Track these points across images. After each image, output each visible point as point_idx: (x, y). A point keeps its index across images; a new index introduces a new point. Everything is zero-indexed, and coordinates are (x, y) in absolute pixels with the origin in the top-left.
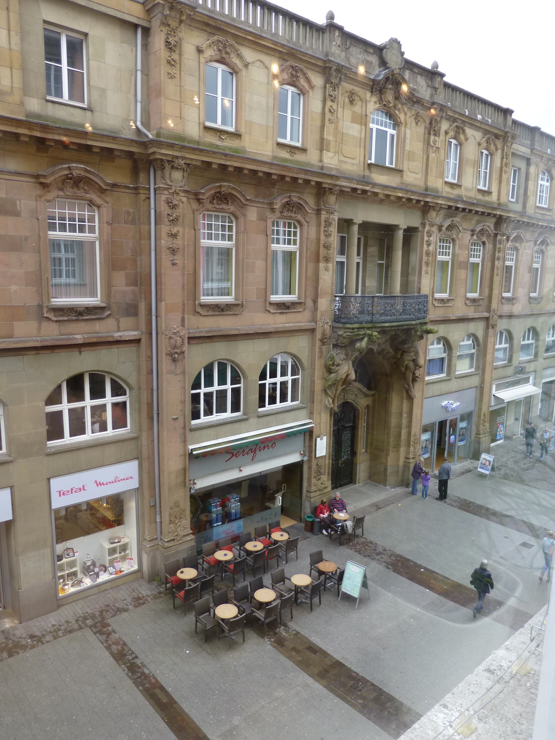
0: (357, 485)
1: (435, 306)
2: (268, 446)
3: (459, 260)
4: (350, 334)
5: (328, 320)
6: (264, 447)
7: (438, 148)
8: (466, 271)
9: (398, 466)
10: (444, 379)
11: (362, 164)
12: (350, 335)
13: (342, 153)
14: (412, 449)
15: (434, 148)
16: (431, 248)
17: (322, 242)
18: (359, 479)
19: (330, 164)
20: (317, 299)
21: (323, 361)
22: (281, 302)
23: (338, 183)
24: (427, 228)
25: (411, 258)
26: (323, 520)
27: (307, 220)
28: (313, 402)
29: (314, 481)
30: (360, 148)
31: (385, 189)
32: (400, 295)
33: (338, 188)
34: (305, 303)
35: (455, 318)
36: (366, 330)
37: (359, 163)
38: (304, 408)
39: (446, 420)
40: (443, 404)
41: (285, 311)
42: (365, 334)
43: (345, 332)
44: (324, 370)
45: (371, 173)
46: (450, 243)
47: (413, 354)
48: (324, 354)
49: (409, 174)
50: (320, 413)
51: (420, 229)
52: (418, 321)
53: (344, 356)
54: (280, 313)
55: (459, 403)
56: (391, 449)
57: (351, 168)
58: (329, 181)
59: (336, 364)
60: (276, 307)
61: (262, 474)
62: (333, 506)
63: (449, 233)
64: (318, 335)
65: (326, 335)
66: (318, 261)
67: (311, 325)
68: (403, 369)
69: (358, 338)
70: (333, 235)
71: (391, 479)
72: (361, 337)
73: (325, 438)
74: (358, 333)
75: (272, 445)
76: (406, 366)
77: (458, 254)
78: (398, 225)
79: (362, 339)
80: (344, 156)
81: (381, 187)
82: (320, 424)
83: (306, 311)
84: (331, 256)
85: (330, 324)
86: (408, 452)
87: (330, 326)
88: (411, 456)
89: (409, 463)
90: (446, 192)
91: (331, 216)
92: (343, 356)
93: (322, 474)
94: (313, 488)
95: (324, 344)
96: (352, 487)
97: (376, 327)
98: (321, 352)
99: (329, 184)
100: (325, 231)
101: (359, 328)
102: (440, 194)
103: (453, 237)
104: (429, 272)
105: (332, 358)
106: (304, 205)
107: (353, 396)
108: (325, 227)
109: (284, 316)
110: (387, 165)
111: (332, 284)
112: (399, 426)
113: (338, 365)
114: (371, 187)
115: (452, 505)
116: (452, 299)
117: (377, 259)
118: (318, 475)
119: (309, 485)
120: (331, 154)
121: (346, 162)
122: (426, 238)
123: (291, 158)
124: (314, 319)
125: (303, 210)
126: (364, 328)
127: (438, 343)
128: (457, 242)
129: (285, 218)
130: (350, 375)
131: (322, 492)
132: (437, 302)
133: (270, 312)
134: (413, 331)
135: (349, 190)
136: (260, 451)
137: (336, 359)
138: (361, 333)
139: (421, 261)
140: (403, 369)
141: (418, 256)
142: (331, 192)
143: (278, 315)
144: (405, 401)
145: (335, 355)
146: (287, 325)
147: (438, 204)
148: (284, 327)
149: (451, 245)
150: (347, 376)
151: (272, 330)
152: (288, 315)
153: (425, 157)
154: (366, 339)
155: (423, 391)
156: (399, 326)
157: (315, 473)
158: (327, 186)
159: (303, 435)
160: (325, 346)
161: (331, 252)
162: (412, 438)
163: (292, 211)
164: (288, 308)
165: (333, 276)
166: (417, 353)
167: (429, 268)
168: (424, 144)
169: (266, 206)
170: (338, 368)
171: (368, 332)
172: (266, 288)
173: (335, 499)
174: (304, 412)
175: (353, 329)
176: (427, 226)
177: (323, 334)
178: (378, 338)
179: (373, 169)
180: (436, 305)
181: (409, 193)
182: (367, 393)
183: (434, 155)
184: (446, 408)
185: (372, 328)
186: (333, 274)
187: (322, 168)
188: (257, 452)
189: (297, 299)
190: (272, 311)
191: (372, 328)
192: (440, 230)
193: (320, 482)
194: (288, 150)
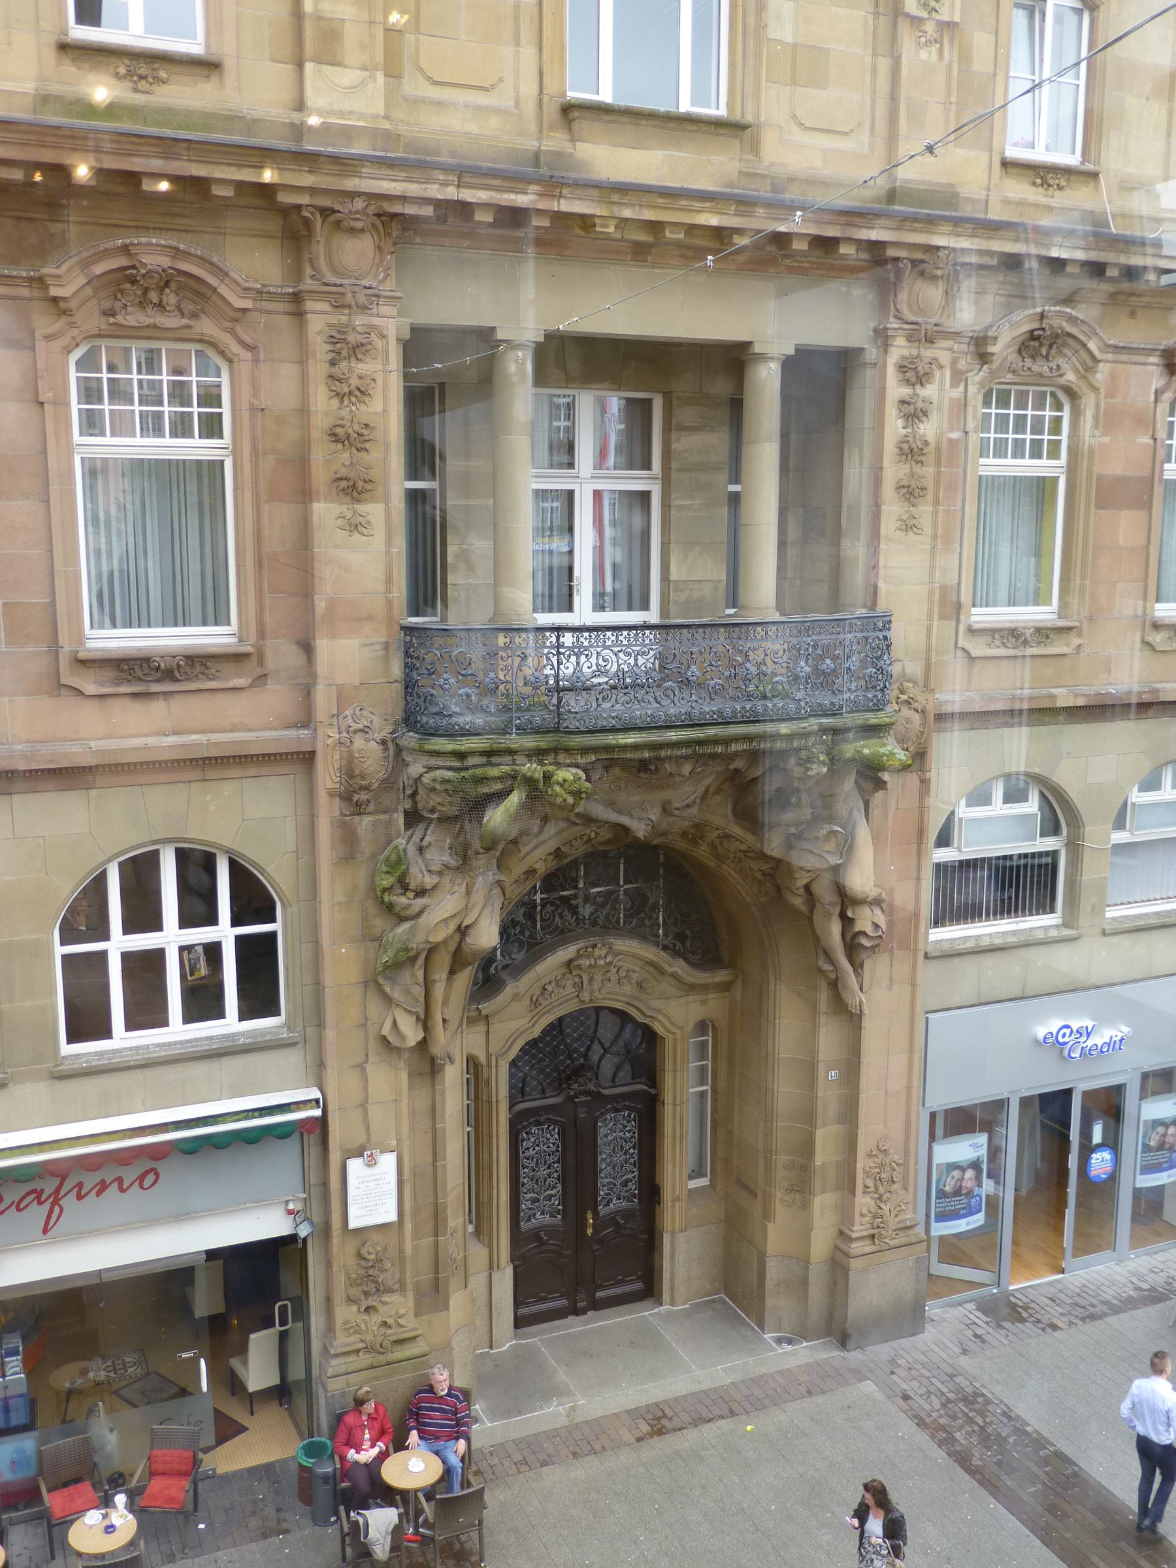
0: (665, 1308)
1: (971, 659)
2: (120, 1180)
3: (1097, 470)
4: (450, 774)
5: (377, 722)
6: (103, 1187)
7: (948, 26)
8: (1143, 514)
9: (806, 1263)
10: (1053, 933)
11: (530, 107)
12: (449, 781)
13: (420, 69)
14: (863, 1202)
15: (930, 27)
16: (928, 429)
17: (320, 422)
18: (672, 1288)
19: (342, 114)
20: (314, 639)
21: (362, 875)
22: (135, 654)
23: (351, 184)
24: (900, 349)
25: (845, 472)
26: (347, 1470)
27: (247, 339)
28: (320, 1024)
29: (344, 1313)
30: (517, 43)
31: (616, 197)
32: (777, 617)
33: (359, 204)
34: (261, 655)
35: (1081, 702)
36: (519, 759)
37: (517, 104)
38: (293, 1045)
39: (1068, 1093)
40: (1041, 1032)
41: (155, 688)
42: (513, 776)
43: (430, 769)
44: (372, 908)
45: (573, 140)
46: (1058, 406)
47: (831, 846)
48: (366, 847)
49: (798, 136)
50: (361, 1067)
51: (871, 354)
52: (812, 724)
53: (446, 858)
54: (135, 696)
55: (1125, 1029)
56: (779, 1194)
57: (472, 128)
58: (307, 180)
59: (412, 886)
60: (110, 674)
61: (106, 1278)
62: (417, 1420)
63: (1040, 366)
64: (327, 776)
65: (363, 776)
66: (305, 494)
67: (291, 738)
68: (798, 902)
69: (486, 790)
70: (377, 391)
71: (777, 1303)
72: (497, 787)
73: (388, 1163)
74: (479, 771)
75: (142, 1178)
76: (807, 888)
77: (1091, 451)
78: (749, 344)
79: (502, 795)
80: (429, 79)
81: (595, 193)
82: (364, 1105)
83: (271, 685)
84: (374, 474)
85: (385, 733)
86: (846, 1213)
87: (383, 742)
88: (859, 1228)
89: (848, 1256)
90: (1007, 202)
91: (359, 321)
92: (439, 857)
93: (390, 1291)
94: (342, 1341)
95: (359, 809)
96: (646, 1313)
97: (568, 750)
98: (348, 840)
99: (312, 191)
100: (331, 377)
101: (489, 754)
102: (966, 211)
103: (1062, 381)
104: (925, 522)
105: (398, 867)
106: (212, 280)
107: (627, 988)
108: (333, 363)
109: (158, 708)
110: (685, 106)
111: (389, 581)
112: (808, 1116)
113: (421, 893)
114: (540, 195)
115: (963, 1460)
116: (1070, 629)
117: (724, 476)
118: (366, 1294)
119: (330, 1328)
120: (346, 77)
121: (441, 104)
122: (895, 390)
123: (140, 99)
124: (306, 721)
125: (214, 298)
126: (511, 752)
127: (1012, 797)
128: (1089, 403)
129: (136, 333)
130: (472, 931)
131: (382, 1359)
132: (982, 640)
133: (79, 693)
134: (792, 762)
135: (428, 211)
136: (80, 1197)
137: (414, 870)
138: (494, 772)
139: (877, 482)
140: (798, 902)
141: (866, 463)
142: (338, 224)
143: (127, 702)
144: (823, 1019)
145: (412, 850)
146: (152, 741)
147: (938, 248)
148: (146, 747)
149: (1066, 414)
150: (463, 931)
151: (90, 761)
152: (177, 703)
153: (884, 64)
154: (515, 798)
155: (913, 985)
156: (701, 743)
157: (352, 1283)
158: (304, 200)
159: (296, 1136)
160: (366, 820)
161: (374, 456)
162: (862, 1163)
163: (160, 306)
164: (169, 675)
165: (388, 552)
166: (847, 847)
167: (925, 510)
168: (876, 15)
169: (25, 292)
170: (420, 902)
171: (531, 768)
172: (53, 604)
173: (431, 1389)
174: (293, 1060)
175: (461, 755)
176: (900, 341)
177: (349, 771)
178: (577, 794)
179: (583, 125)
180: (976, 652)
181: (760, 211)
182: (689, 979)
183: (928, 55)
184: (1054, 1044)
185: (556, 750)
186: (389, 542)
187: (299, 131)
188: (69, 1202)
189: (233, 640)
190: (91, 688)
191: (556, 750)
192: (984, 358)
193: (375, 1319)
194: (122, 70)
